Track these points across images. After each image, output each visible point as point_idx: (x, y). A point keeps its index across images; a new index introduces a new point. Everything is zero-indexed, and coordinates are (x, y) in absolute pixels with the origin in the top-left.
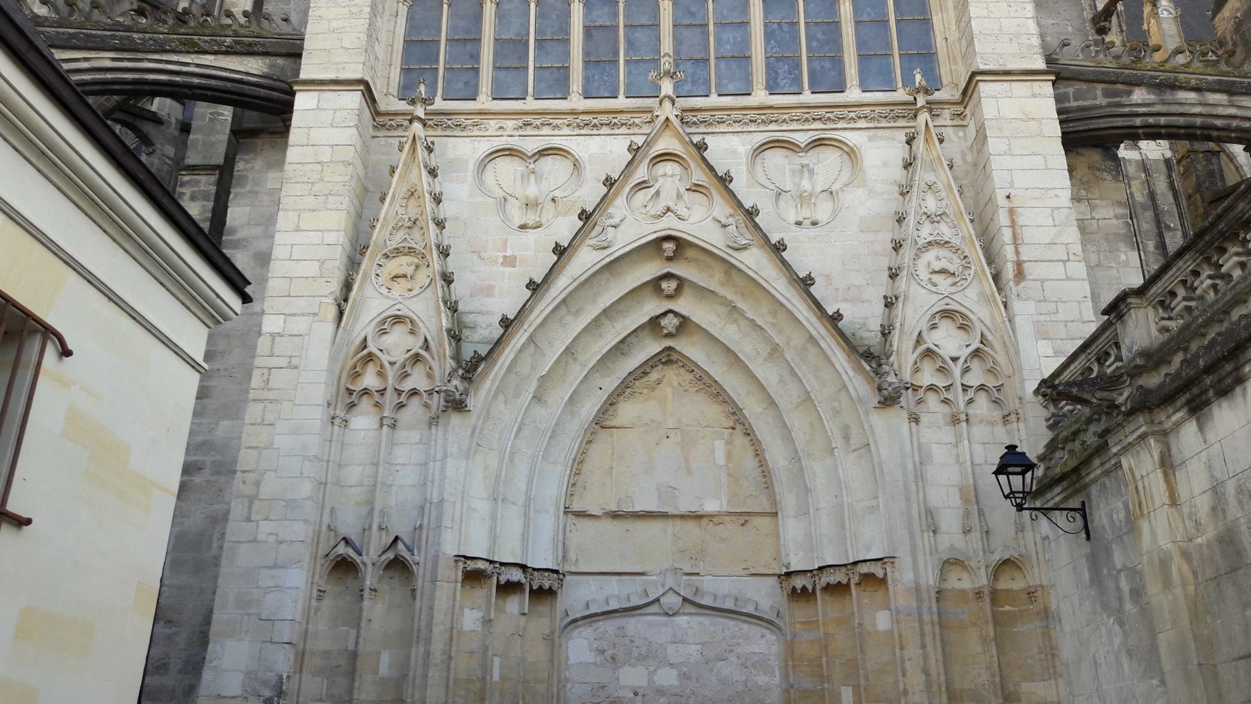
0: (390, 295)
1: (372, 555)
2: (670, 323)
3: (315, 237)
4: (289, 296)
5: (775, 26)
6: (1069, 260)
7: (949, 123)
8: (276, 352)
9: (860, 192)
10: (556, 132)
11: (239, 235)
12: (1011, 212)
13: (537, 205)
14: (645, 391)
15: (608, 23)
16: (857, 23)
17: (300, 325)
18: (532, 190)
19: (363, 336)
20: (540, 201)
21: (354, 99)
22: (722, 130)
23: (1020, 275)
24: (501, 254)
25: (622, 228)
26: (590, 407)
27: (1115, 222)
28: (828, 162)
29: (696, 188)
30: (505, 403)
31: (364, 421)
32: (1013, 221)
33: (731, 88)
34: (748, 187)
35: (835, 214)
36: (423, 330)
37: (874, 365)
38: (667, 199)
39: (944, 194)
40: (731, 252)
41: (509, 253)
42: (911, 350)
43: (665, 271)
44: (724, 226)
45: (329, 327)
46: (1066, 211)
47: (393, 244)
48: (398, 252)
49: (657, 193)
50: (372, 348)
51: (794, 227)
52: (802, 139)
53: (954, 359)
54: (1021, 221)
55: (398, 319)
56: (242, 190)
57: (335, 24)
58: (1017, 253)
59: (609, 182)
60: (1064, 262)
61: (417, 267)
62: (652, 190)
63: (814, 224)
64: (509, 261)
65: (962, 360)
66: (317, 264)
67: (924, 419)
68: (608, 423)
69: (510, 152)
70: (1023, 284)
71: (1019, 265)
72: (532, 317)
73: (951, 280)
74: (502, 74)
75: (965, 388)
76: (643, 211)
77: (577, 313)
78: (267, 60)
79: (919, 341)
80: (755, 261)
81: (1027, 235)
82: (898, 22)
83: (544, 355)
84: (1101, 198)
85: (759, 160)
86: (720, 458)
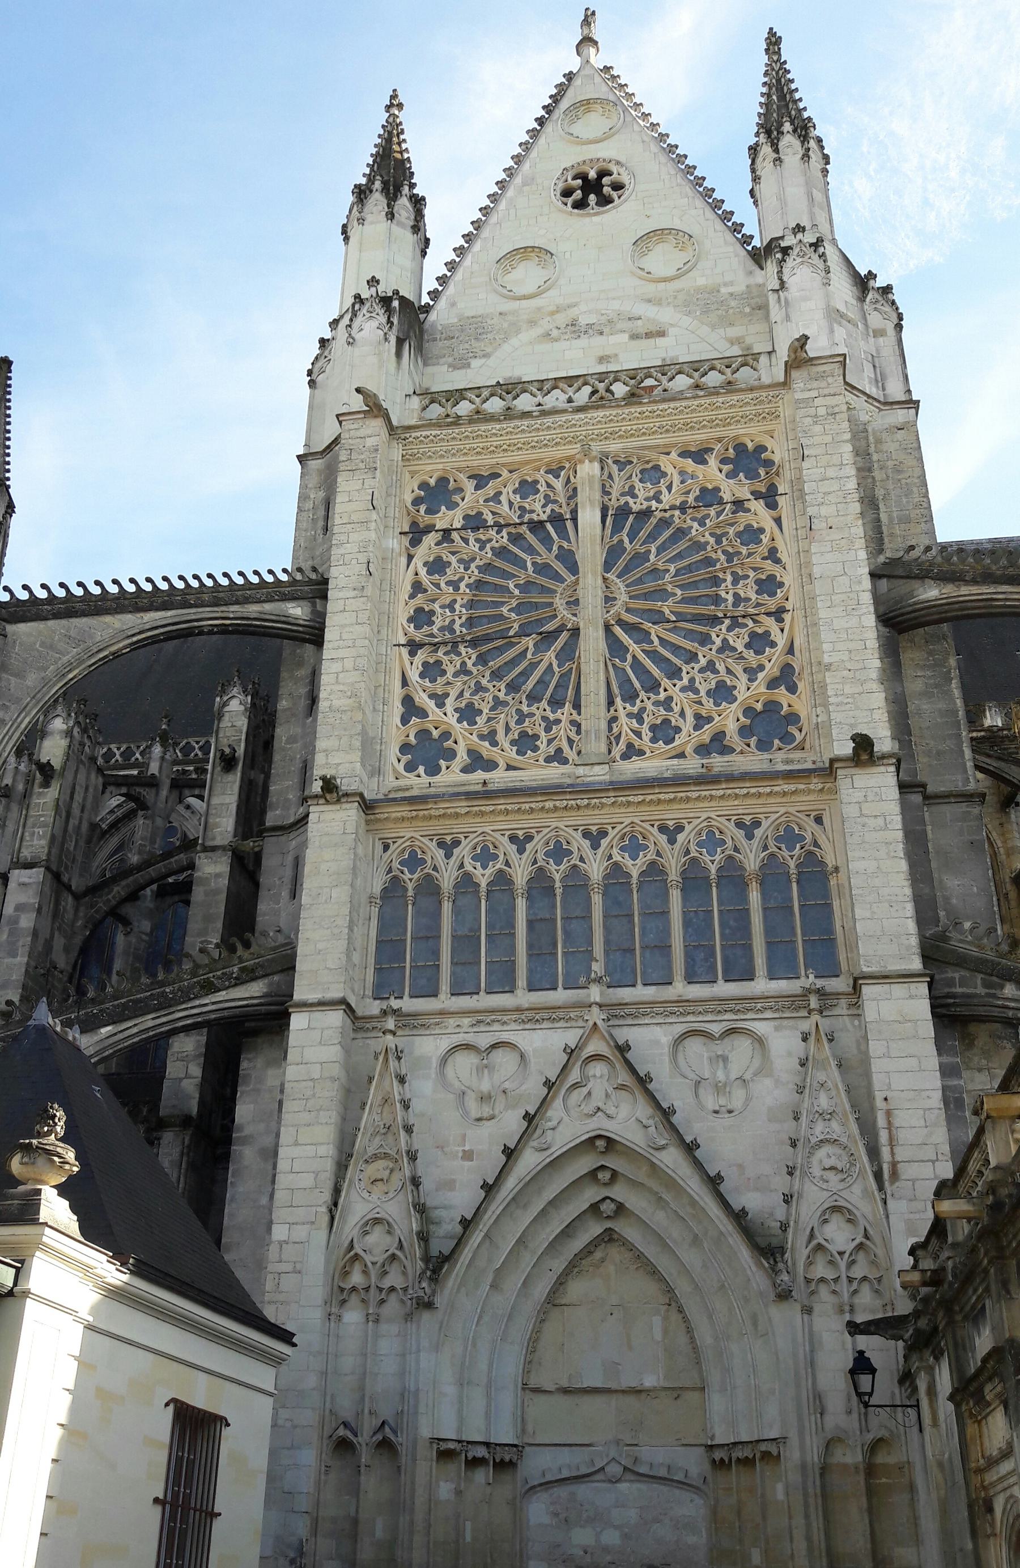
1: (365, 1439)
2: (607, 1208)
3: (310, 1150)
4: (291, 1206)
5: (692, 914)
6: (937, 1160)
7: (845, 1012)
8: (284, 1257)
9: (768, 1082)
10: (505, 1028)
11: (247, 1132)
13: (490, 1098)
14: (591, 1269)
15: (548, 916)
16: (765, 909)
17: (300, 1233)
18: (485, 1086)
20: (493, 1094)
21: (336, 1018)
22: (647, 1022)
23: (895, 1175)
25: (560, 1128)
26: (541, 1290)
28: (740, 1050)
29: (622, 1087)
31: (353, 1316)
32: (889, 1123)
33: (655, 977)
35: (748, 1099)
37: (772, 1262)
38: (597, 1100)
39: (834, 1093)
40: (652, 1151)
41: (467, 1148)
43: (599, 1164)
44: (645, 1127)
45: (323, 1234)
46: (937, 1111)
47: (371, 1151)
48: (376, 1157)
49: (589, 1093)
50: (358, 1249)
51: (711, 1117)
52: (716, 1029)
53: (841, 1254)
54: (897, 1122)
55: (377, 1221)
57: (320, 946)
58: (893, 1154)
59: (549, 1085)
60: (933, 1162)
61: (392, 1171)
62: (585, 1091)
63: (730, 1112)
64: (468, 1156)
65: (847, 1255)
67: (817, 1308)
68: (557, 1302)
69: (467, 1047)
70: (897, 1184)
71: (894, 1165)
72: (486, 1217)
73: (840, 1176)
74: (459, 969)
75: (850, 1280)
77: (525, 1207)
79: (812, 1236)
80: (672, 1159)
81: (902, 1136)
82: (801, 906)
85: (681, 1048)
86: (658, 1335)
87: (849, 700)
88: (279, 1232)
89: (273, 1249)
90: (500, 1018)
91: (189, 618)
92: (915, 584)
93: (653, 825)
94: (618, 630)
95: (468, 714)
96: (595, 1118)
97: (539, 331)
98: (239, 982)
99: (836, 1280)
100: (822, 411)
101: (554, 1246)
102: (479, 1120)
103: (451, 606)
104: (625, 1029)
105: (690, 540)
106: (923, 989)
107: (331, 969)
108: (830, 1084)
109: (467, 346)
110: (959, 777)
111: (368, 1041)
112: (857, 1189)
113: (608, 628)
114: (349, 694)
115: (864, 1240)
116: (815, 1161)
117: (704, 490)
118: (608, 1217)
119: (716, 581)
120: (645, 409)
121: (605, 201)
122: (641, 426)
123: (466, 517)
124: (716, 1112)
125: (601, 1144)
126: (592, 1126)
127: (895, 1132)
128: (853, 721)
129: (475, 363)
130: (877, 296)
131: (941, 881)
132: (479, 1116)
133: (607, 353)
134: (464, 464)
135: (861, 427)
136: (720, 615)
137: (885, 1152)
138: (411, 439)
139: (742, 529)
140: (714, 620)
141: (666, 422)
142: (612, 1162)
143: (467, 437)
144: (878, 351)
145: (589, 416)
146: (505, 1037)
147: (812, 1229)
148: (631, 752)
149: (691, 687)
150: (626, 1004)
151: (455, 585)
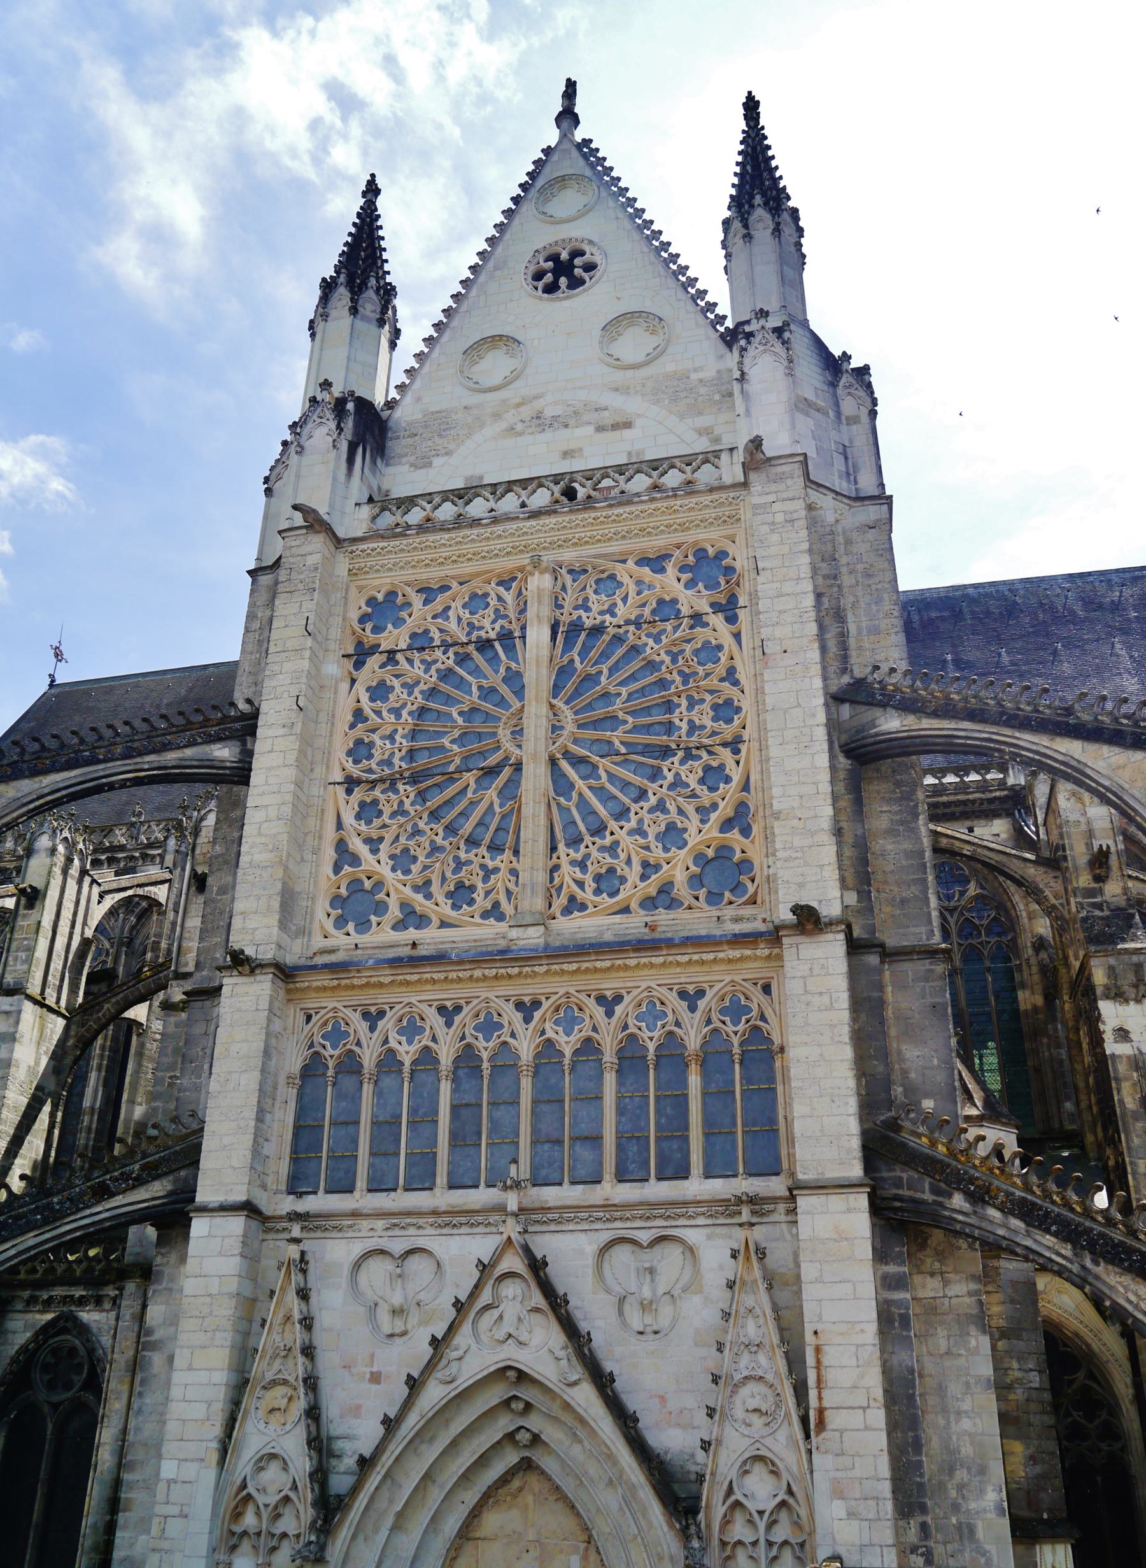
0: (266, 1431)
2: (524, 1437)
3: (202, 1377)
4: (182, 1440)
5: (627, 1100)
7: (783, 1218)
8: (172, 1499)
9: (697, 1299)
10: (421, 1232)
11: (156, 1336)
12: (818, 1350)
14: (508, 1498)
15: (473, 1101)
16: (705, 1094)
17: (190, 1471)
18: (397, 1299)
19: (243, 1476)
20: (405, 1307)
22: (571, 1228)
23: (821, 1424)
24: (368, 1369)
25: (467, 1358)
26: (452, 1524)
27: (967, 1300)
28: (670, 1260)
29: (536, 1310)
30: (365, 1540)
32: (818, 1361)
33: (582, 1173)
34: (594, 1293)
35: (675, 1320)
36: (292, 1470)
37: (684, 1523)
38: (507, 1327)
39: (761, 1320)
40: (563, 1387)
41: (375, 1369)
42: (734, 1484)
43: (511, 1394)
45: (210, 1475)
46: (870, 1348)
47: (269, 1376)
48: (274, 1383)
49: (501, 1317)
52: (644, 1237)
53: (761, 1513)
54: (826, 1361)
55: (273, 1456)
56: (160, 1287)
57: (227, 1140)
58: (820, 1398)
59: (458, 1305)
61: (290, 1399)
62: (495, 1313)
63: (656, 1333)
64: (375, 1378)
65: (766, 1515)
66: (204, 1406)
70: (823, 1435)
71: (821, 1411)
72: (384, 1458)
73: (764, 1419)
74: (377, 1161)
75: (770, 1544)
76: (489, 1334)
77: (432, 1439)
78: (171, 1178)
79: (730, 1491)
80: (586, 1397)
81: (830, 1376)
82: (743, 1091)
83: (400, 1486)
84: (955, 1271)
85: (607, 1256)
87: (798, 855)
88: (168, 1469)
89: (162, 1487)
90: (415, 1221)
91: (96, 775)
92: (877, 712)
93: (589, 996)
94: (564, 765)
95: (402, 861)
96: (505, 1346)
97: (504, 425)
98: (139, 1182)
99: (755, 1543)
100: (780, 518)
101: (466, 1477)
102: (391, 1336)
103: (391, 737)
104: (547, 1236)
105: (644, 659)
106: (861, 1201)
107: (235, 1169)
108: (758, 1311)
109: (430, 443)
110: (923, 929)
111: (278, 1243)
112: (782, 1435)
113: (553, 761)
114: (271, 847)
115: (786, 1497)
116: (738, 1399)
117: (660, 602)
118: (525, 1446)
119: (669, 706)
120: (599, 514)
121: (576, 283)
122: (595, 533)
123: (413, 636)
124: (641, 1333)
125: (511, 1374)
126: (502, 1356)
127: (823, 1372)
128: (801, 879)
129: (437, 462)
130: (851, 379)
131: (899, 1052)
132: (389, 1332)
133: (571, 447)
134: (412, 578)
135: (828, 529)
136: (674, 746)
137: (813, 1394)
138: (358, 552)
139: (699, 645)
140: (666, 752)
141: (622, 528)
142: (527, 1393)
143: (415, 548)
144: (851, 441)
145: (541, 522)
146: (421, 1242)
147: (731, 1482)
148: (574, 905)
149: (639, 831)
150: (549, 1208)
151: (397, 712)
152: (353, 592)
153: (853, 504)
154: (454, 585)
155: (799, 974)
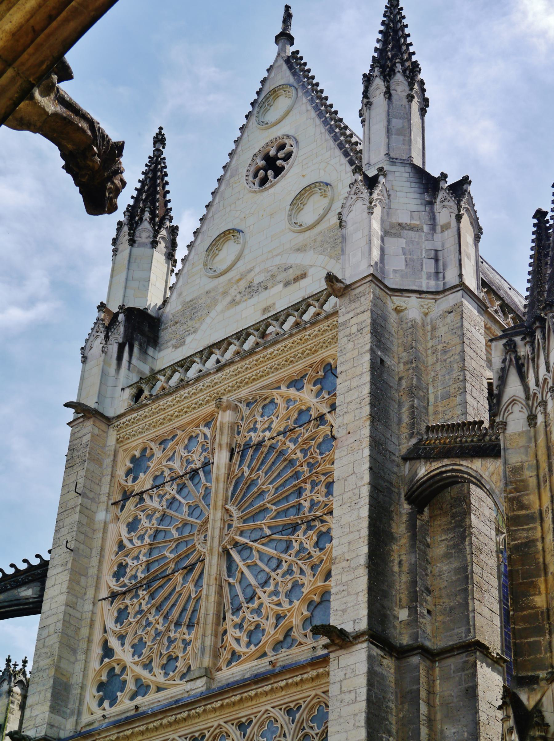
87: (345, 588)
94: (234, 554)
95: (137, 649)
97: (229, 299)
100: (354, 329)
103: (137, 558)
105: (285, 460)
109: (185, 327)
110: (463, 629)
113: (226, 553)
114: (49, 654)
117: (301, 412)
119: (299, 491)
120: (258, 356)
123: (155, 478)
128: (343, 607)
129: (188, 339)
130: (446, 195)
131: (442, 731)
133: (268, 304)
134: (153, 435)
135: (410, 324)
136: (299, 522)
138: (121, 425)
139: (321, 440)
140: (295, 527)
141: (274, 363)
143: (153, 413)
144: (443, 246)
145: (224, 373)
149: (276, 593)
151: (141, 538)
152: (121, 454)
153: (437, 297)
154: (179, 432)
155: (338, 680)
